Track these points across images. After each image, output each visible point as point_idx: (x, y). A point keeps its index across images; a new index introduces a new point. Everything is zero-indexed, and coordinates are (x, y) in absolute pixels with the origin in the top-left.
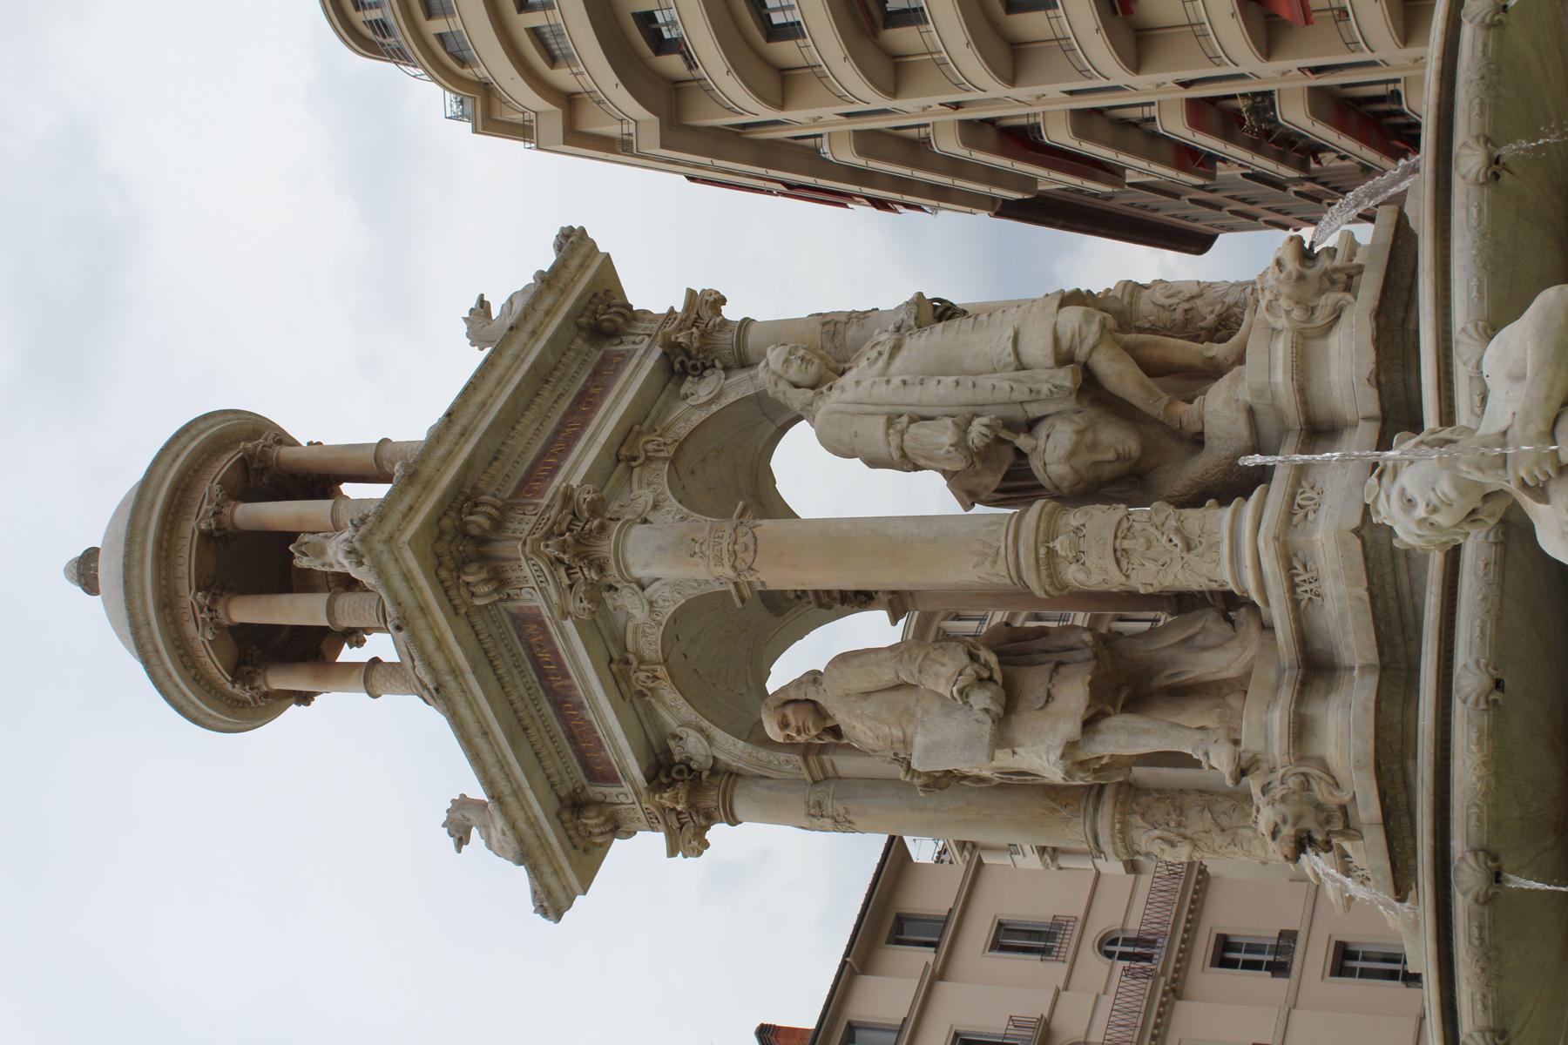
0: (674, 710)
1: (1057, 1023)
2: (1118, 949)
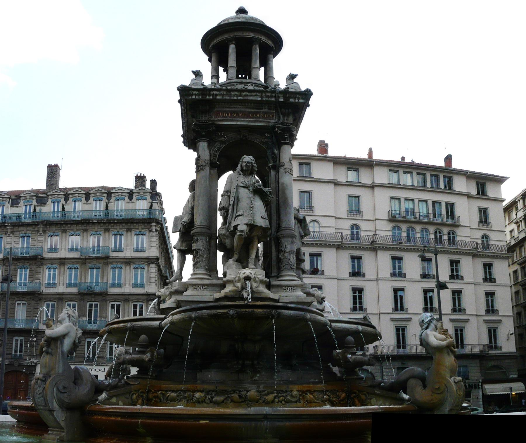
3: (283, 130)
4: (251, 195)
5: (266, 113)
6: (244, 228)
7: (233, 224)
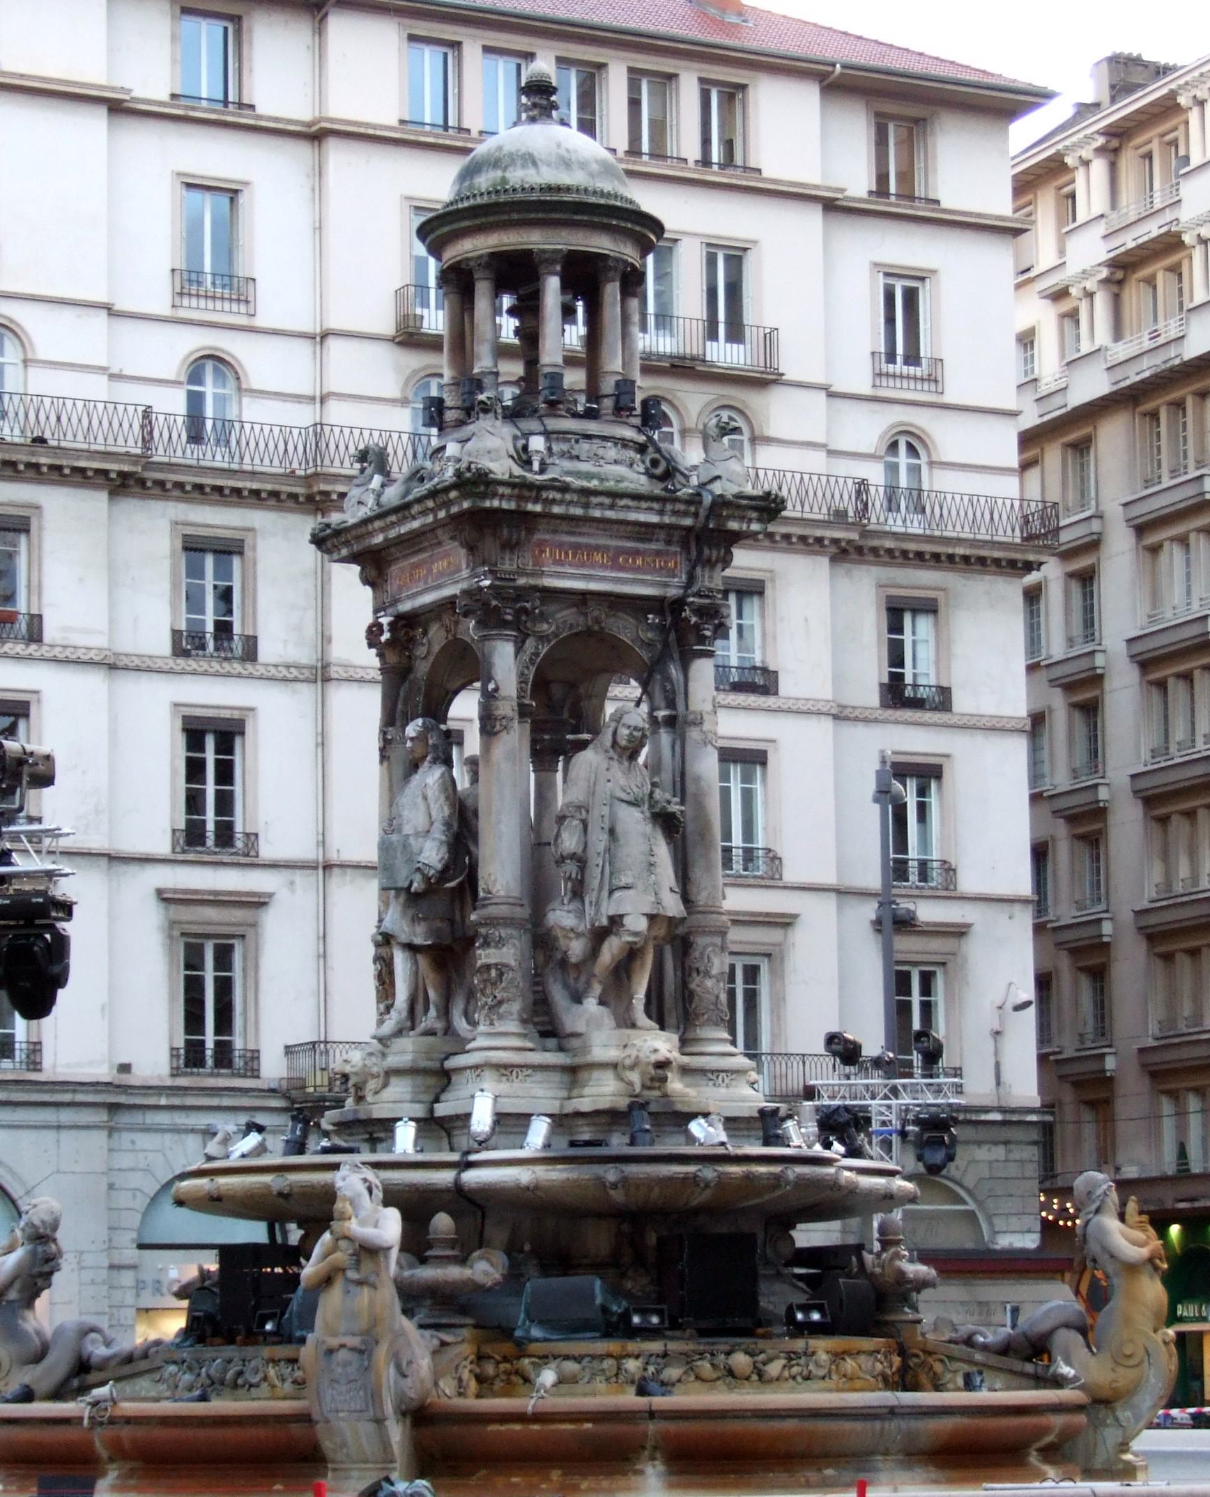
0: (436, 637)
1: (777, 393)
2: (903, 459)
3: (700, 611)
4: (648, 828)
5: (658, 553)
6: (642, 925)
7: (610, 908)
